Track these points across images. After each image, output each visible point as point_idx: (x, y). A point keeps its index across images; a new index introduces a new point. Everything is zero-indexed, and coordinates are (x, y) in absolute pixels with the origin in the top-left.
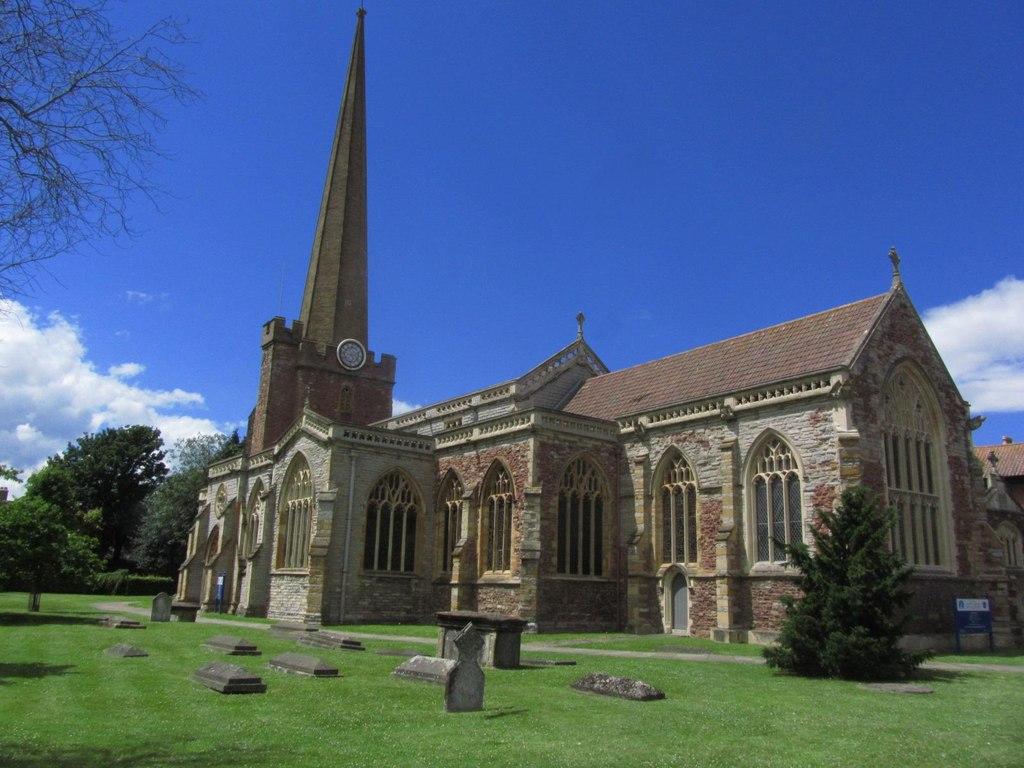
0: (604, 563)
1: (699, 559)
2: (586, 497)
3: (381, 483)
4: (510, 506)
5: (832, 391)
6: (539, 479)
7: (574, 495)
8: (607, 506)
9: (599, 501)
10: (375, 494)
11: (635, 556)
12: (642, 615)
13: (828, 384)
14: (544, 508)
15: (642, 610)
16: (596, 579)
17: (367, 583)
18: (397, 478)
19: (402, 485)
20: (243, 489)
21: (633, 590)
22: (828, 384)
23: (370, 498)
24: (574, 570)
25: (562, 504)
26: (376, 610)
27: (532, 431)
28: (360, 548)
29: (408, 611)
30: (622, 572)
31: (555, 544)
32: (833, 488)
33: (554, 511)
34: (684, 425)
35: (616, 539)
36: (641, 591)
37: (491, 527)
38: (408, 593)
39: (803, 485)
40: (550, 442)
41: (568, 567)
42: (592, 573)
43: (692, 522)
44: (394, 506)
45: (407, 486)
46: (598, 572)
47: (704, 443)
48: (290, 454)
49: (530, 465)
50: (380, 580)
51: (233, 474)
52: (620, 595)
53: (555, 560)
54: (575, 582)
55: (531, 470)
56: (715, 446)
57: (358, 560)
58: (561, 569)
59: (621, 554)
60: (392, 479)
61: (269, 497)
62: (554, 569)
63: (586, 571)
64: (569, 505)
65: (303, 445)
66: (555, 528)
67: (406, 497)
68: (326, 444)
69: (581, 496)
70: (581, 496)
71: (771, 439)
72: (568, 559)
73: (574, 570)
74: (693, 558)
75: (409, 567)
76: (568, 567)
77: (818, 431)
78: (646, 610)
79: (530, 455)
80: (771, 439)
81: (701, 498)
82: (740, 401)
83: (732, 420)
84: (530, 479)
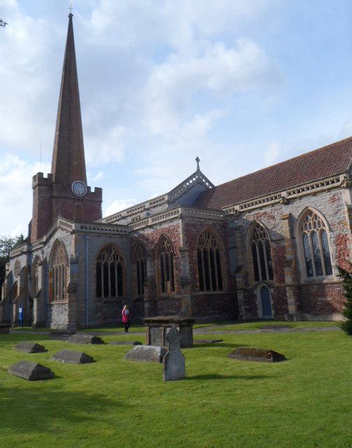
0: (223, 284)
1: (275, 278)
2: (211, 250)
3: (102, 251)
5: (341, 184)
6: (186, 243)
8: (222, 254)
9: (217, 251)
10: (99, 257)
11: (239, 280)
12: (246, 309)
13: (338, 181)
15: (246, 307)
17: (99, 304)
18: (111, 249)
19: (113, 252)
20: (29, 260)
21: (240, 297)
22: (338, 181)
23: (98, 259)
25: (199, 254)
26: (105, 318)
27: (181, 217)
28: (94, 287)
30: (233, 287)
32: (346, 235)
33: (195, 258)
34: (261, 208)
36: (245, 297)
37: (162, 270)
39: (329, 234)
40: (191, 223)
42: (218, 289)
43: (269, 259)
44: (110, 263)
45: (116, 252)
46: (221, 288)
47: (273, 218)
48: (52, 241)
49: (181, 236)
50: (105, 302)
51: (23, 253)
52: (234, 299)
53: (198, 284)
54: (210, 295)
55: (181, 238)
56: (278, 217)
57: (93, 293)
58: (202, 289)
59: (232, 278)
60: (108, 248)
61: (44, 264)
64: (203, 255)
65: (59, 235)
66: (196, 267)
67: (116, 258)
68: (73, 232)
69: (208, 251)
70: (208, 251)
71: (307, 213)
72: (205, 283)
73: (208, 289)
74: (271, 278)
75: (120, 293)
77: (335, 205)
78: (249, 307)
79: (180, 230)
80: (307, 213)
81: (273, 245)
82: (290, 194)
83: (288, 202)
84: (182, 243)
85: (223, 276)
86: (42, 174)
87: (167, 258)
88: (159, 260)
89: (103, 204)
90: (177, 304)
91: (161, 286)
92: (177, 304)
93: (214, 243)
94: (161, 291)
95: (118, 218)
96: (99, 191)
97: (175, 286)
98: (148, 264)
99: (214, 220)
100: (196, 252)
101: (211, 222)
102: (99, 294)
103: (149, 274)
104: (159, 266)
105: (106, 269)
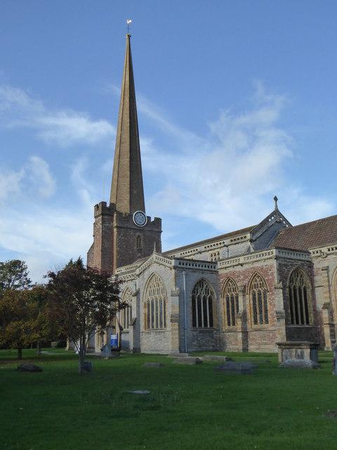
4: (265, 294)
7: (294, 287)
14: (284, 293)
16: (307, 326)
17: (195, 333)
24: (297, 323)
29: (213, 346)
31: (289, 311)
35: (314, 307)
38: (212, 337)
41: (295, 321)
46: (308, 323)
50: (200, 332)
53: (290, 318)
54: (299, 328)
55: (276, 277)
57: (190, 323)
58: (293, 323)
62: (289, 323)
63: (303, 323)
66: (288, 303)
69: (297, 288)
72: (295, 318)
75: (211, 325)
76: (295, 321)
79: (275, 270)
84: (276, 281)
85: (309, 311)
86: (105, 203)
87: (260, 294)
88: (251, 296)
89: (162, 235)
90: (271, 335)
91: (253, 319)
92: (271, 335)
93: (302, 281)
94: (253, 323)
95: (194, 253)
96: (158, 221)
97: (269, 319)
98: (240, 299)
99: (303, 261)
100: (288, 289)
101: (300, 263)
102: (194, 325)
103: (241, 308)
104: (251, 302)
105: (199, 302)
